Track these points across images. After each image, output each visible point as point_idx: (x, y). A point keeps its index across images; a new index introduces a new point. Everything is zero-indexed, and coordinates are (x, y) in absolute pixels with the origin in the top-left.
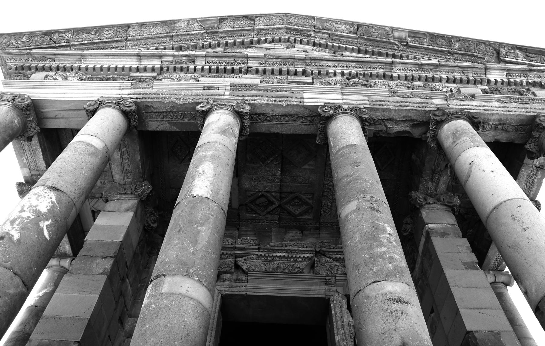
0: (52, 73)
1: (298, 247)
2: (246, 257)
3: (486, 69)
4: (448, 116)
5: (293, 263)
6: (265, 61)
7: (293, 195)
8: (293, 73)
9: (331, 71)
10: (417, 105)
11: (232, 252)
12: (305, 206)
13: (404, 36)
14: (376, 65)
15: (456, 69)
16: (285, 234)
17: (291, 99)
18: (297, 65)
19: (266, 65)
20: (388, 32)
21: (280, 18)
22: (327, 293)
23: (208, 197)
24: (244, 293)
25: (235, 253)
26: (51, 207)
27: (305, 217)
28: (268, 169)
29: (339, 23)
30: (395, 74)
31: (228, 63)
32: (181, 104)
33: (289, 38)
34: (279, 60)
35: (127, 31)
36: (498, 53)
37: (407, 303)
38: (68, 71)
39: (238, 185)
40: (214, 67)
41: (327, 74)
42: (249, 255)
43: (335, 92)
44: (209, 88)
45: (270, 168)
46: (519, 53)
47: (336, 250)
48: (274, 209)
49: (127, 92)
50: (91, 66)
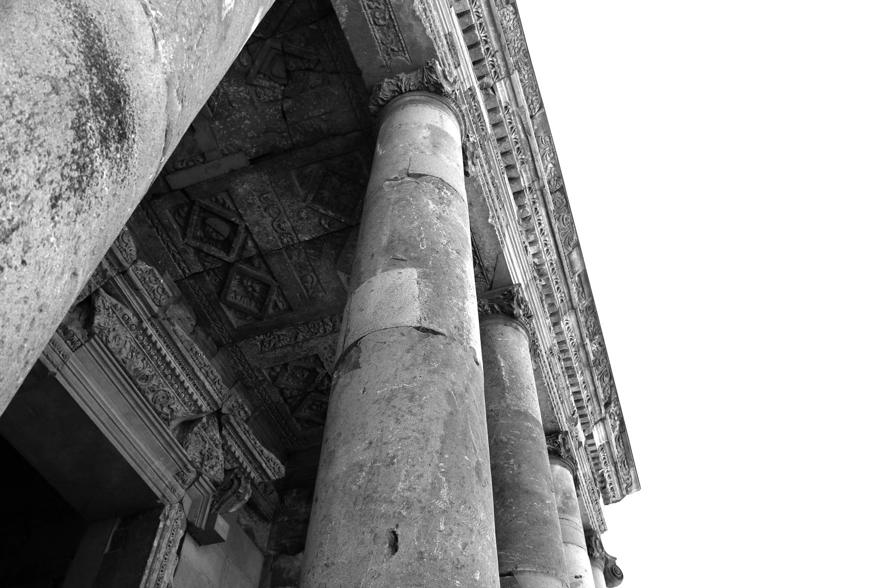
1: (207, 376)
2: (120, 305)
3: (603, 420)
6: (513, 112)
7: (269, 278)
8: (513, 175)
12: (253, 304)
13: (577, 269)
14: (563, 288)
15: (592, 388)
16: (174, 303)
18: (525, 171)
19: (507, 116)
22: (168, 493)
24: (52, 369)
25: (112, 278)
27: (230, 314)
28: (303, 215)
29: (552, 155)
31: (486, 42)
32: (414, 12)
34: (523, 136)
39: (233, 171)
42: (129, 305)
45: (308, 218)
47: (244, 437)
48: (214, 257)
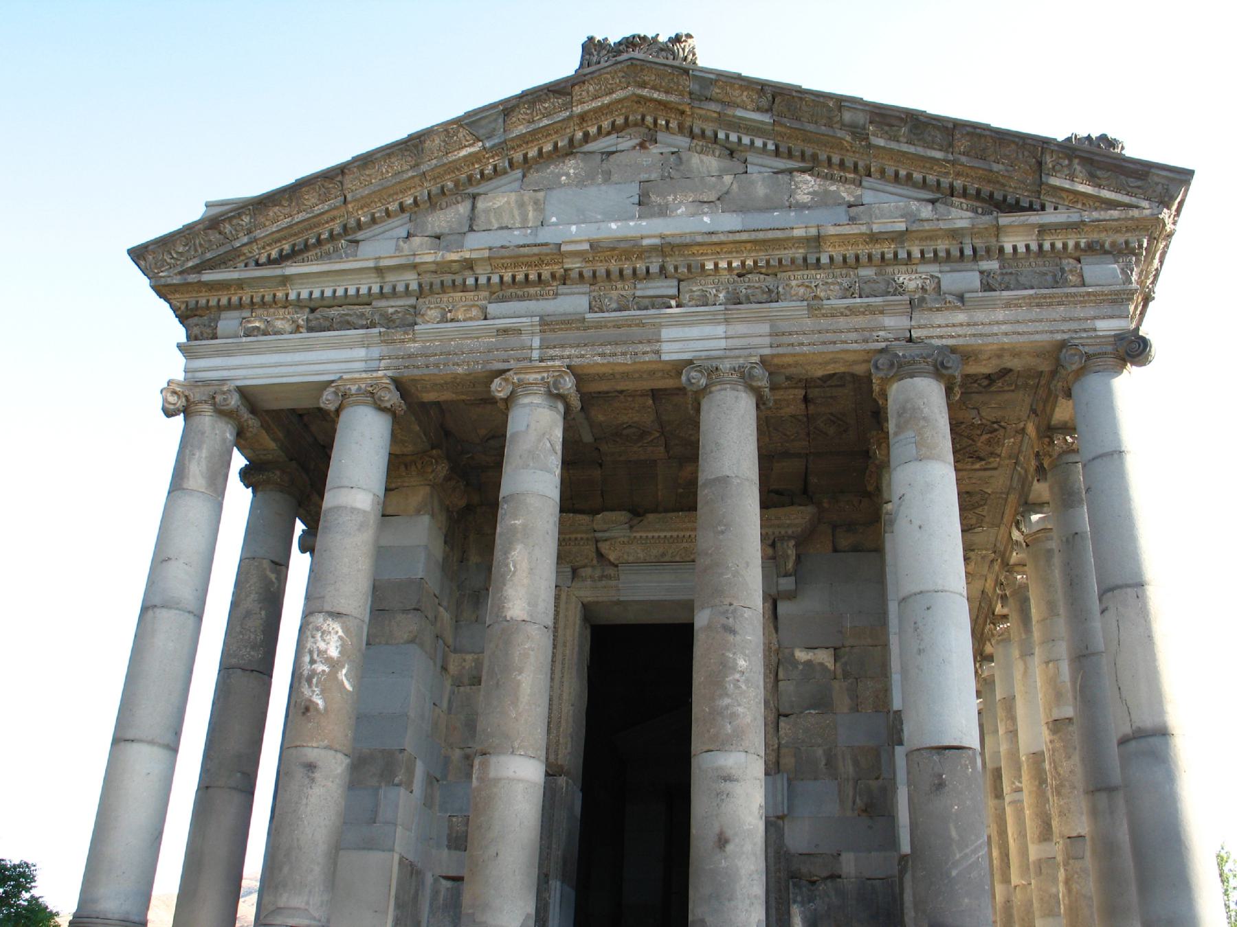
0: (246, 313)
4: (900, 366)
5: (685, 545)
9: (710, 266)
10: (854, 336)
11: (589, 536)
13: (862, 122)
17: (640, 348)
20: (830, 110)
21: (620, 74)
23: (525, 617)
24: (615, 599)
26: (342, 646)
30: (825, 260)
33: (643, 119)
35: (341, 183)
36: (1040, 164)
37: (737, 780)
38: (271, 307)
40: (507, 278)
41: (703, 266)
43: (713, 321)
44: (505, 331)
46: (1078, 168)
49: (376, 352)
50: (304, 295)
